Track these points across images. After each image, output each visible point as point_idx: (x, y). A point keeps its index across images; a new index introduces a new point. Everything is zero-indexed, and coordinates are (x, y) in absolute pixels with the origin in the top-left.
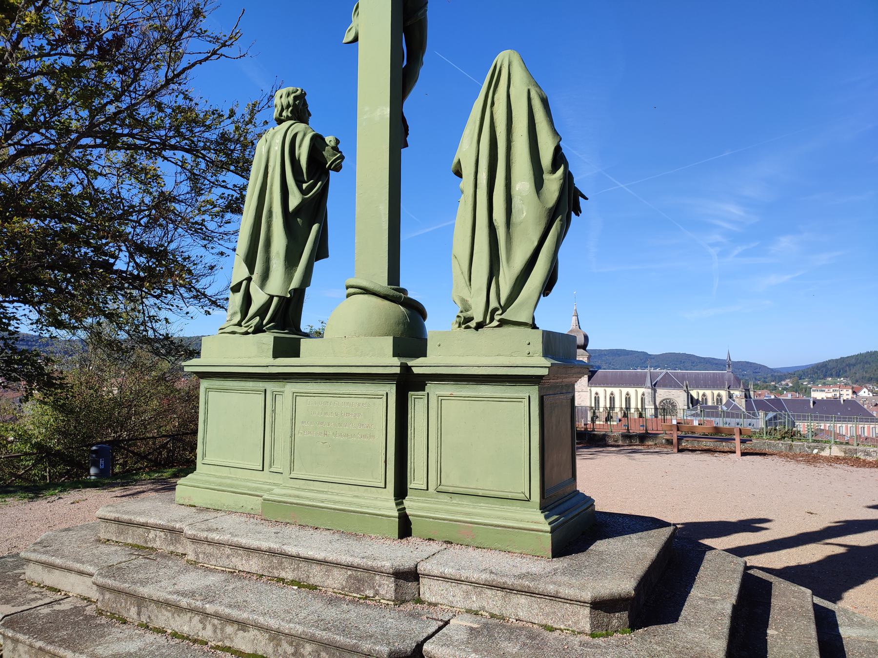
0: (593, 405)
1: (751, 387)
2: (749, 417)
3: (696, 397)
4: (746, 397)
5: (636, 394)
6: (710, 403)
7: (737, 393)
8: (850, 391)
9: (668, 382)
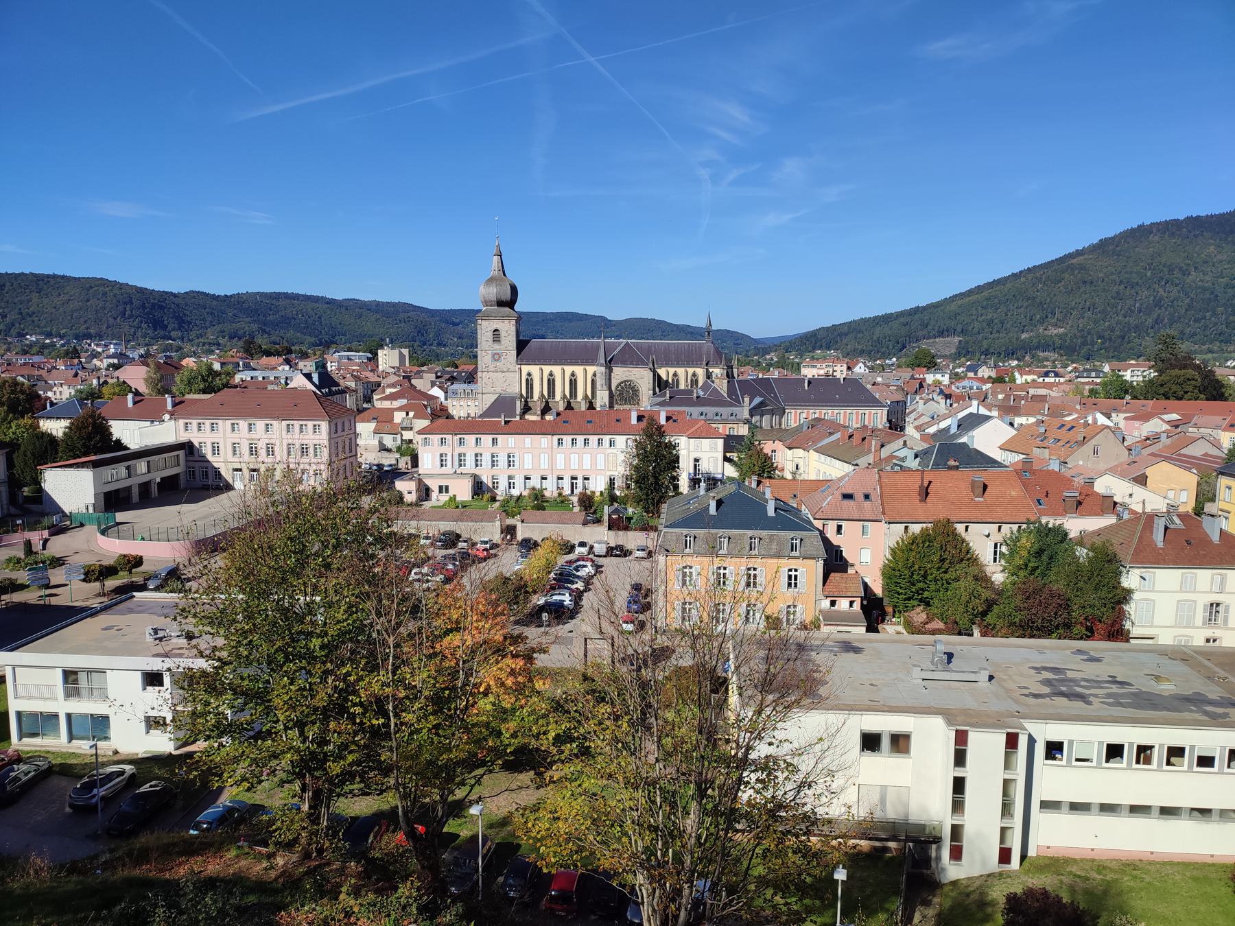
0: (524, 393)
2: (731, 405)
3: (664, 378)
4: (728, 375)
5: (584, 373)
6: (682, 386)
7: (717, 371)
9: (629, 358)
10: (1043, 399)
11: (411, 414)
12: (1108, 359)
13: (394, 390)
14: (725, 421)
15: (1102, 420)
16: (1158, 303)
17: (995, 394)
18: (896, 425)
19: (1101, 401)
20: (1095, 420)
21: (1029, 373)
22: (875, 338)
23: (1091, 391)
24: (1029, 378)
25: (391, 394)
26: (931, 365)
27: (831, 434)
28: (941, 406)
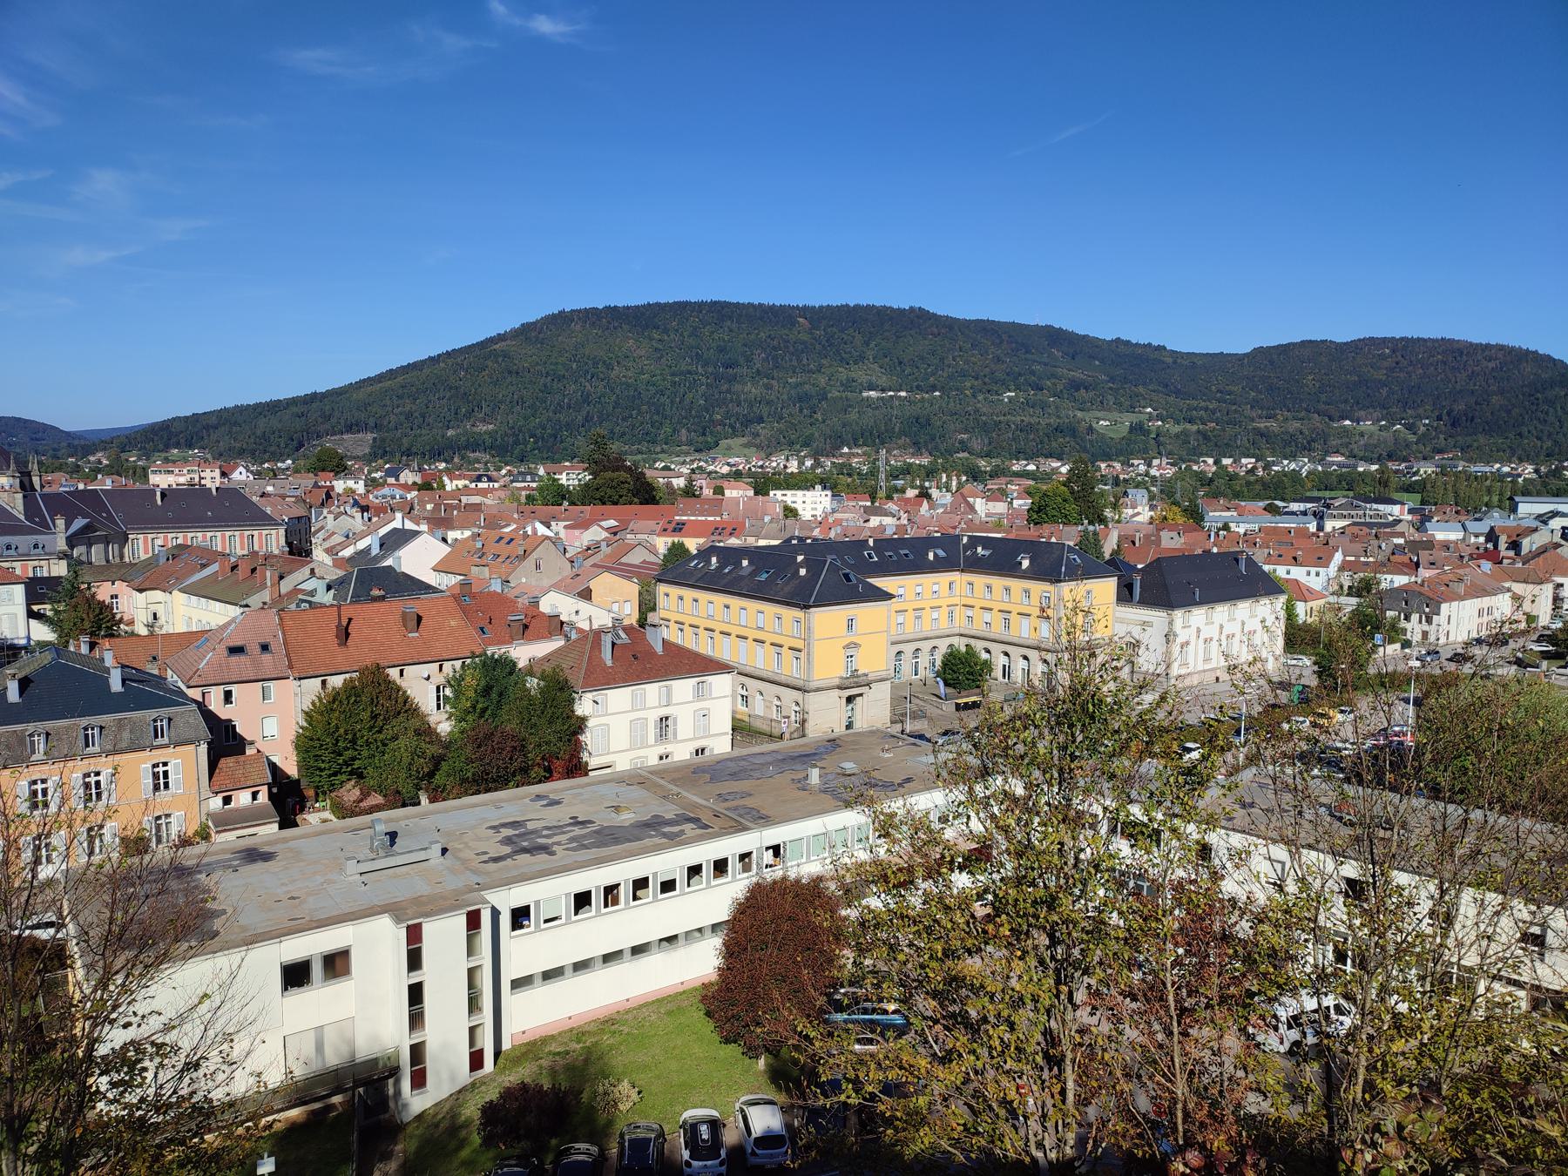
1: (34, 467)
4: (23, 486)
8: (217, 473)
10: (477, 508)
12: (543, 460)
14: (25, 557)
15: (542, 530)
16: (586, 399)
17: (422, 504)
18: (299, 548)
19: (541, 509)
20: (534, 530)
21: (459, 477)
22: (259, 433)
23: (528, 497)
24: (461, 483)
26: (340, 469)
27: (204, 566)
28: (357, 521)
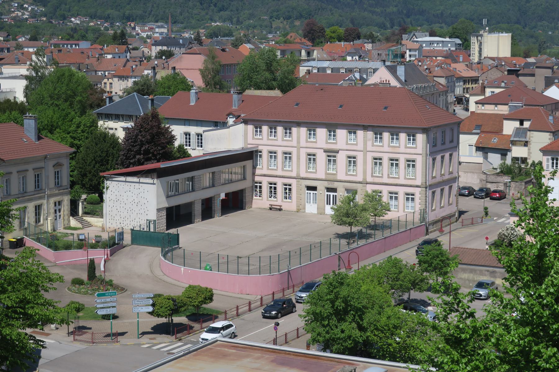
11: (527, 124)
13: (497, 91)
25: (494, 95)
